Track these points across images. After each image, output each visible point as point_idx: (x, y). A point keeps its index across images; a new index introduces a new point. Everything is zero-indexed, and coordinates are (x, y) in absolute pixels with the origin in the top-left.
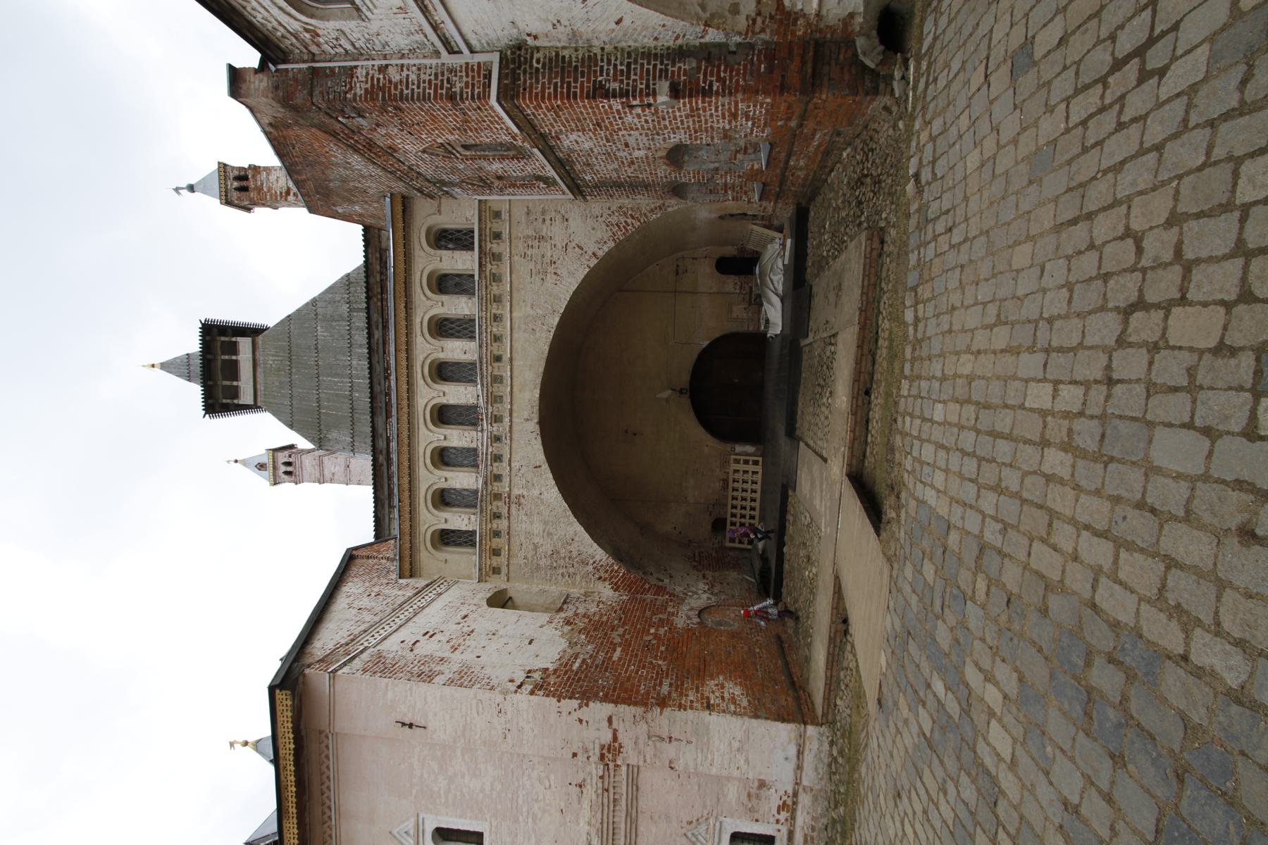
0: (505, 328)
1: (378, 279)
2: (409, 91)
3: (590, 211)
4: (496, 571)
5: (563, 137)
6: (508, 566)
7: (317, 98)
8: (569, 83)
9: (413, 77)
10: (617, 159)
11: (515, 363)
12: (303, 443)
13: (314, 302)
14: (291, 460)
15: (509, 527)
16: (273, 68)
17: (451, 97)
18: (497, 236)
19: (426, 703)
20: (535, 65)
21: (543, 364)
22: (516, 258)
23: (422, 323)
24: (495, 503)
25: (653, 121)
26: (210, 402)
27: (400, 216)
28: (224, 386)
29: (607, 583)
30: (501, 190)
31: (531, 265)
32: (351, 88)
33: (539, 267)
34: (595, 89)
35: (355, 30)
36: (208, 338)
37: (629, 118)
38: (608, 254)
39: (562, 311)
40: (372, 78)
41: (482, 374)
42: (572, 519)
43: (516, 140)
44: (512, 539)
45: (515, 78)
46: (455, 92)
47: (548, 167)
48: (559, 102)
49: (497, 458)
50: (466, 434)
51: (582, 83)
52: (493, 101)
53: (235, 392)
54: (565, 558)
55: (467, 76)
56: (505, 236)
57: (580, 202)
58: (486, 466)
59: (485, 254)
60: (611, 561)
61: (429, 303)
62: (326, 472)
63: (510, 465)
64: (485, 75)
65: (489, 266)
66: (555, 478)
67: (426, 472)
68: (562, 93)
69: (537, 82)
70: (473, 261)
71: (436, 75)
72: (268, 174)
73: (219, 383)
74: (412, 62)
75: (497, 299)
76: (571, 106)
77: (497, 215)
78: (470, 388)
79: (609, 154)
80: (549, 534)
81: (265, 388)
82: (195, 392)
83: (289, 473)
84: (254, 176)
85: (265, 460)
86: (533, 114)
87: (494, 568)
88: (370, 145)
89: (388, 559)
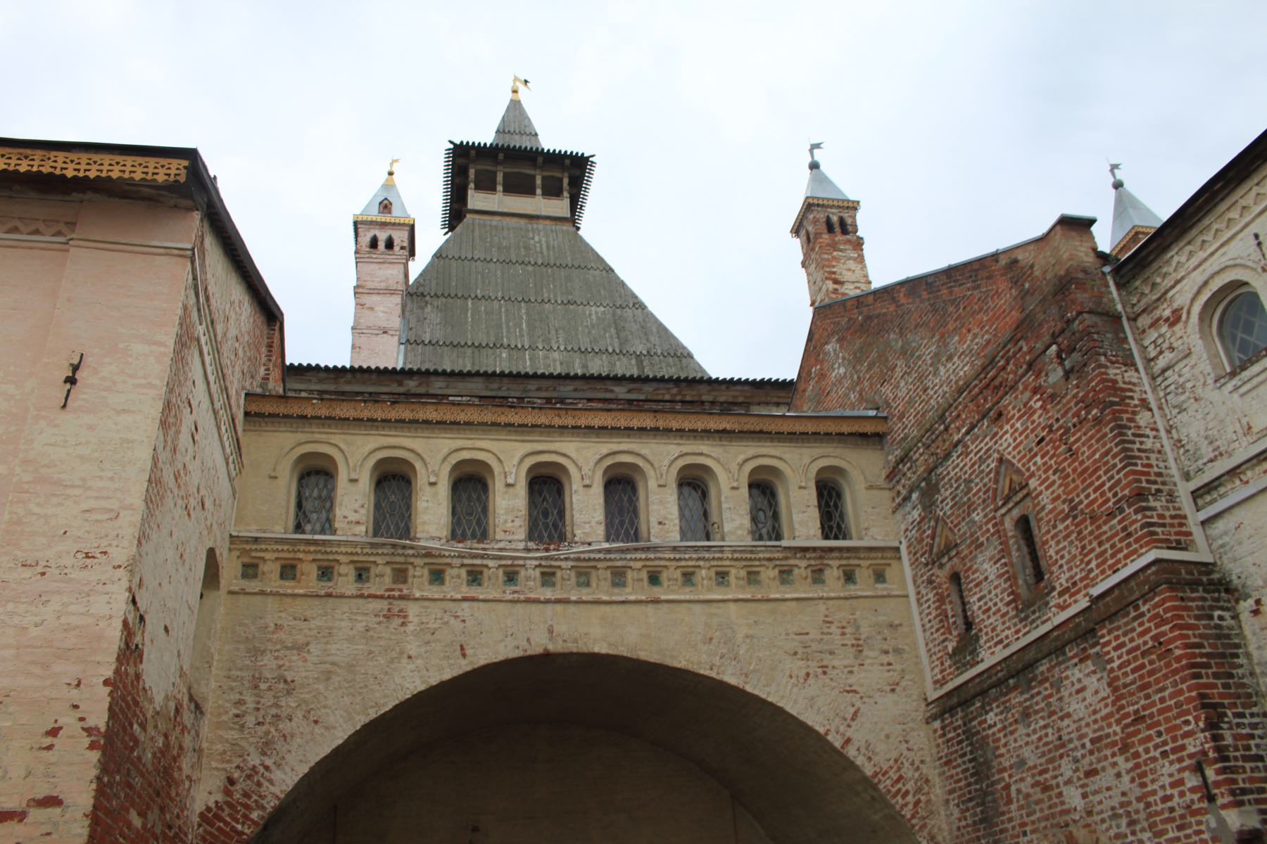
0: (709, 590)
1: (705, 398)
2: (1131, 438)
3: (912, 729)
4: (250, 570)
5: (1090, 666)
6: (262, 593)
7: (1089, 319)
8: (1207, 666)
9: (1149, 444)
10: (1051, 761)
11: (650, 609)
12: (416, 268)
13: (639, 305)
14: (397, 248)
15: (342, 596)
16: (1107, 269)
17: (1140, 495)
18: (849, 577)
19: (119, 412)
20: (1217, 613)
21: (653, 658)
22: (822, 607)
23: (701, 454)
24: (388, 570)
25: (1172, 810)
26: (473, 153)
27: (856, 428)
28: (495, 173)
29: (220, 797)
30: (930, 582)
31: (815, 634)
32: (1112, 362)
33: (815, 646)
34: (1214, 706)
35: (1196, 371)
36: (567, 162)
37: (1167, 769)
38: (852, 765)
39: (749, 689)
40: (1131, 390)
41: (628, 550)
42: (360, 721)
43: (1061, 594)
44: (316, 602)
45: (1194, 584)
46: (1148, 500)
47: (1001, 654)
48: (1178, 652)
49: (475, 576)
50: (518, 522)
51: (1214, 686)
52: (1152, 555)
53: (486, 185)
54: (277, 706)
55: (1172, 517)
56: (852, 590)
57: (921, 712)
58: (461, 556)
59: (821, 558)
60: (270, 804)
61: (734, 467)
62: (375, 298)
63: (465, 599)
64: (1178, 542)
65: (804, 563)
66: (443, 684)
67: (446, 451)
68: (1194, 656)
69: (1198, 618)
70: (808, 538)
71: (1159, 474)
72: (855, 259)
73: (499, 168)
74: (1165, 442)
75: (752, 577)
76: (1176, 672)
77: (880, 577)
78: (601, 531)
79: (1063, 746)
80: (328, 675)
81: (496, 227)
82: (485, 135)
83: (374, 243)
84: (849, 242)
85: (396, 211)
86: (1142, 615)
87: (256, 566)
88: (997, 388)
89: (266, 379)
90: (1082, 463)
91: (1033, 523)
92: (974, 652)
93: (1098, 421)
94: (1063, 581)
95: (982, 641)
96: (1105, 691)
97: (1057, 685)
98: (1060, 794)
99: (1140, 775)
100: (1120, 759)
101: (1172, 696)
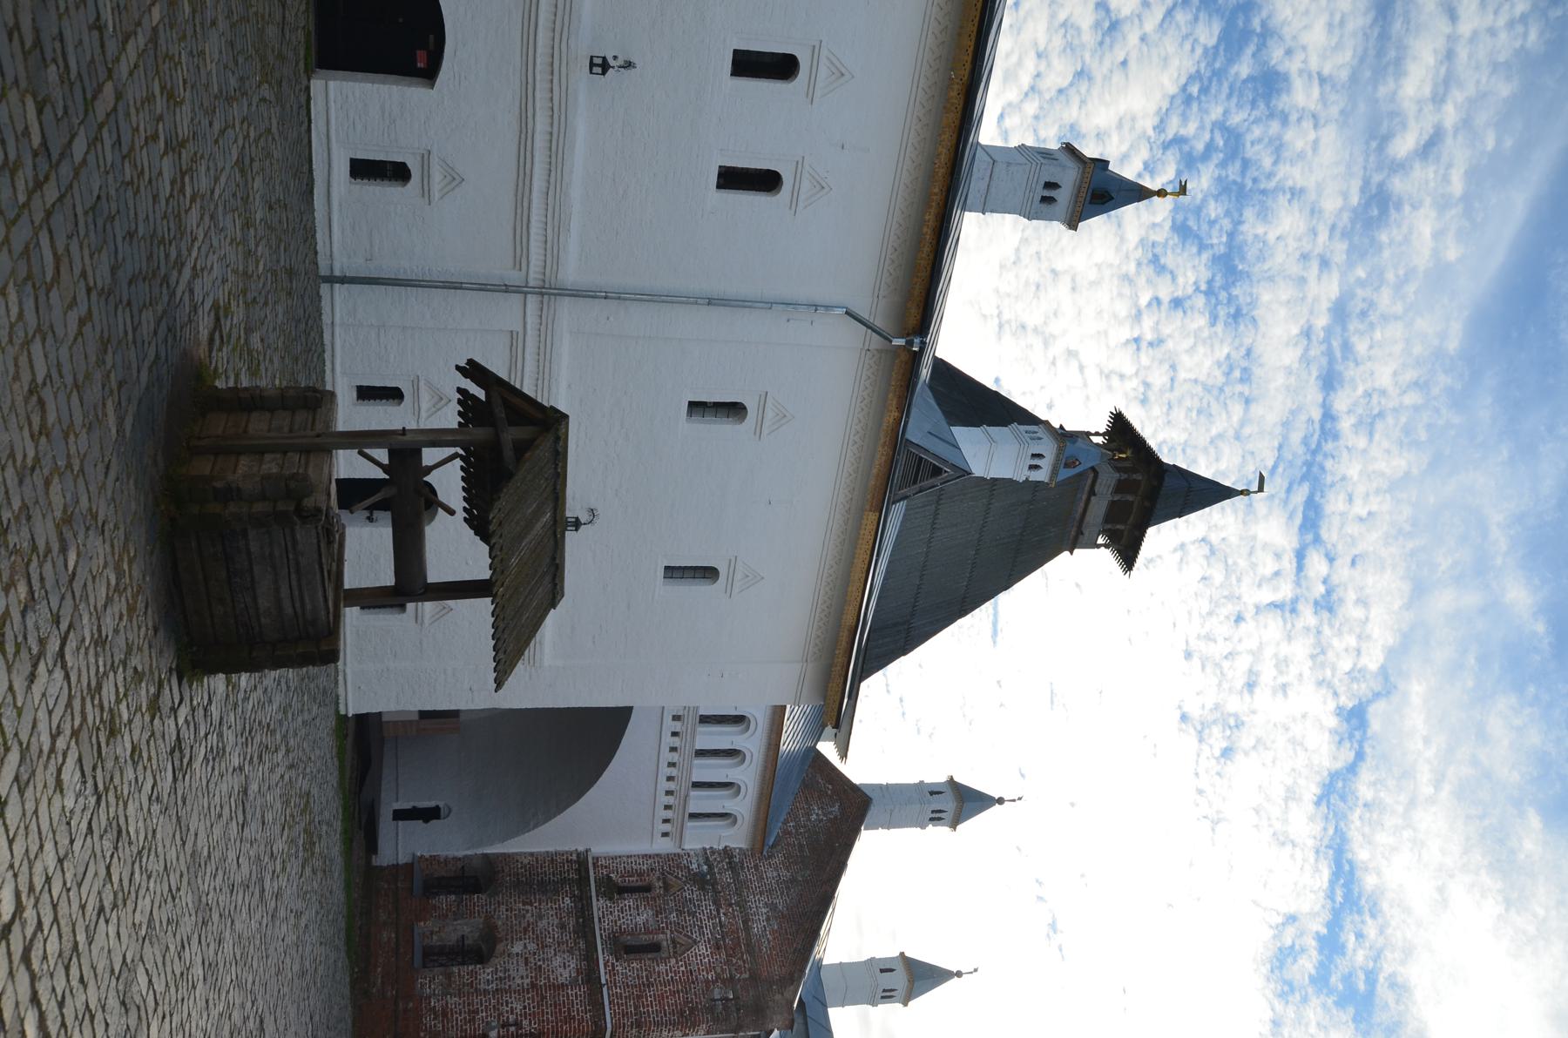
36: (1131, 554)
43: (613, 964)
52: (609, 1025)
56: (658, 821)
90: (667, 997)
91: (655, 955)
92: (604, 895)
93: (682, 1013)
94: (619, 968)
95: (608, 902)
96: (561, 980)
97: (571, 951)
98: (521, 940)
99: (521, 991)
100: (529, 980)
101: (548, 1019)
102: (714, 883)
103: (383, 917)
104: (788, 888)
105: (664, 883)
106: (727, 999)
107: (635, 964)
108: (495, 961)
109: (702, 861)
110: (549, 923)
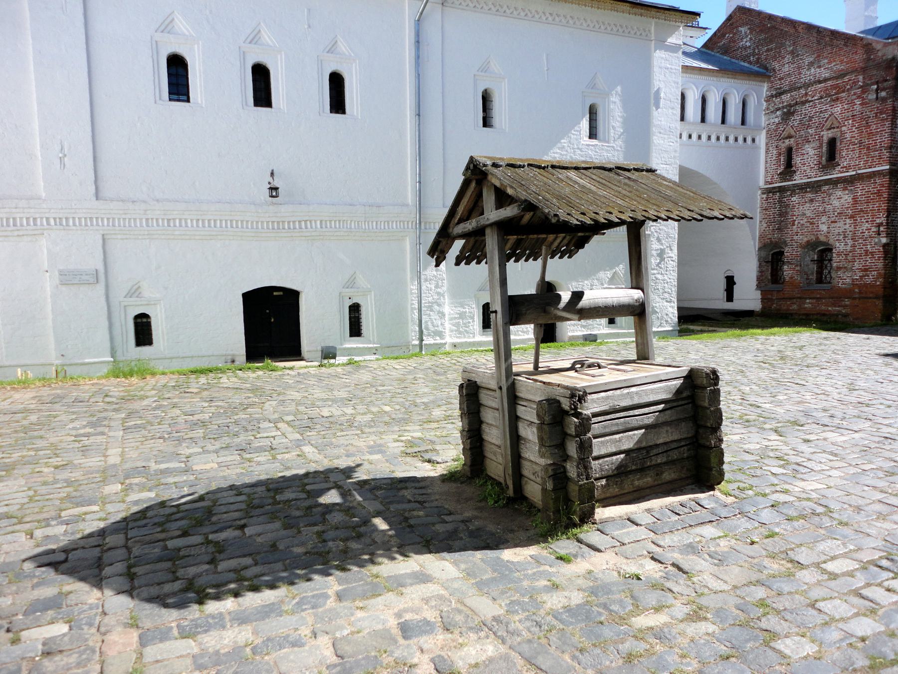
95: (797, 174)
96: (850, 200)
102: (790, 106)
103: (795, 307)
104: (797, 56)
105: (786, 138)
106: (877, 90)
107: (844, 154)
108: (831, 241)
109: (774, 116)
110: (808, 210)
